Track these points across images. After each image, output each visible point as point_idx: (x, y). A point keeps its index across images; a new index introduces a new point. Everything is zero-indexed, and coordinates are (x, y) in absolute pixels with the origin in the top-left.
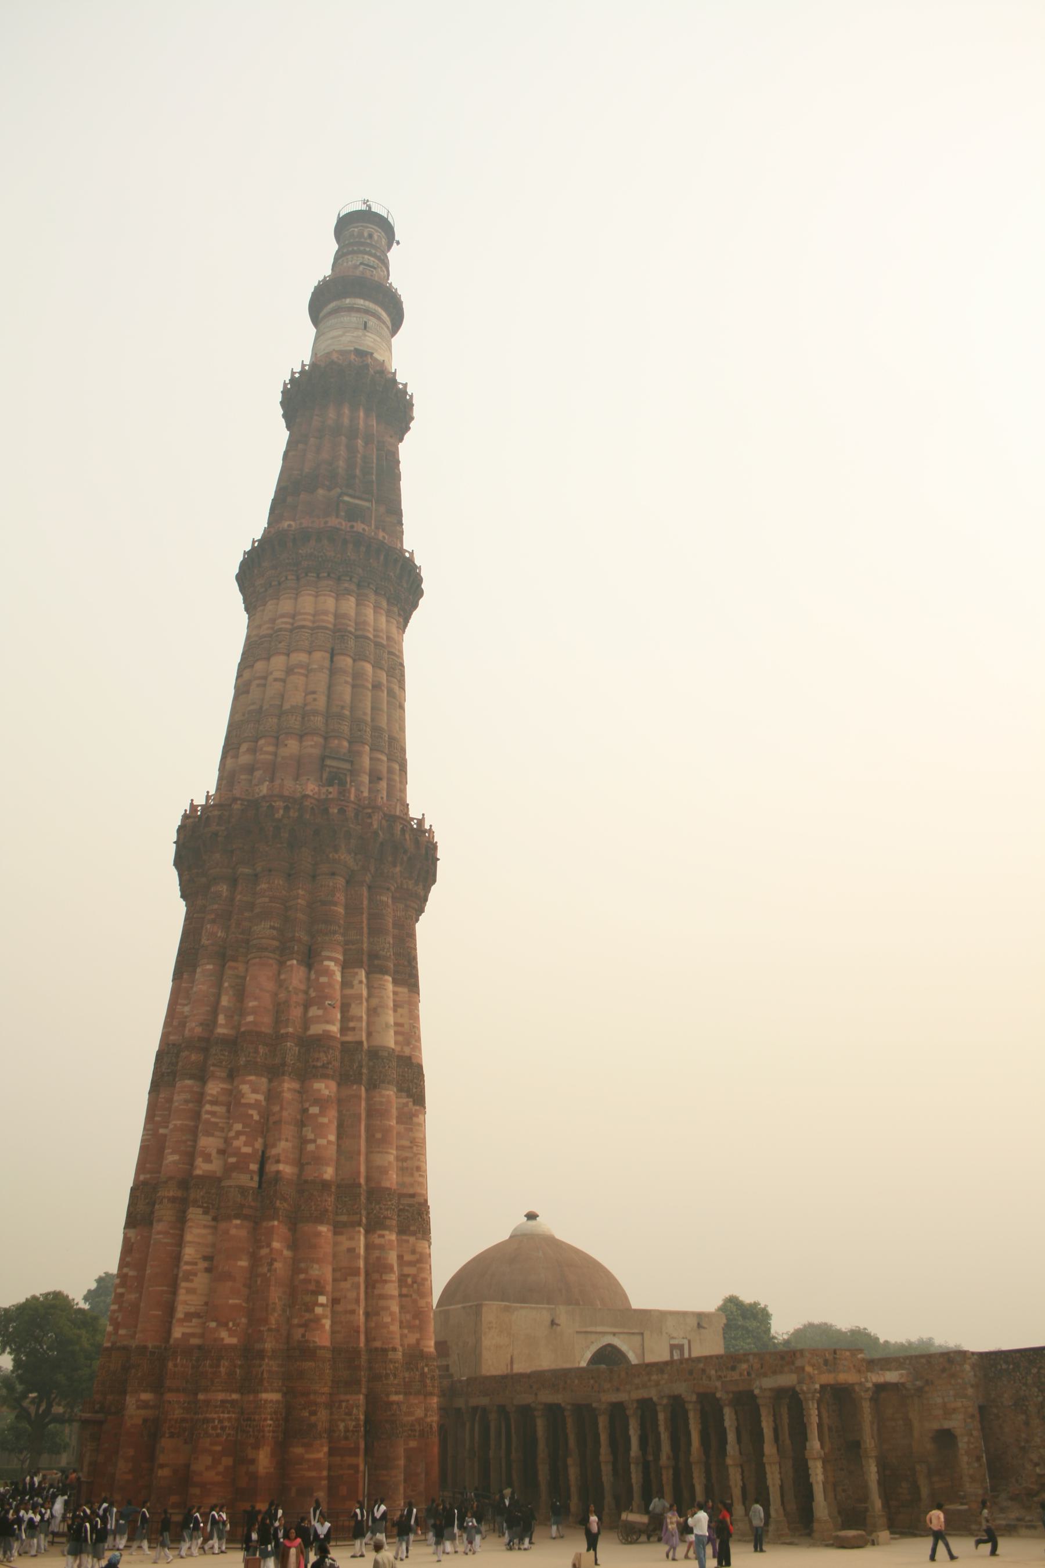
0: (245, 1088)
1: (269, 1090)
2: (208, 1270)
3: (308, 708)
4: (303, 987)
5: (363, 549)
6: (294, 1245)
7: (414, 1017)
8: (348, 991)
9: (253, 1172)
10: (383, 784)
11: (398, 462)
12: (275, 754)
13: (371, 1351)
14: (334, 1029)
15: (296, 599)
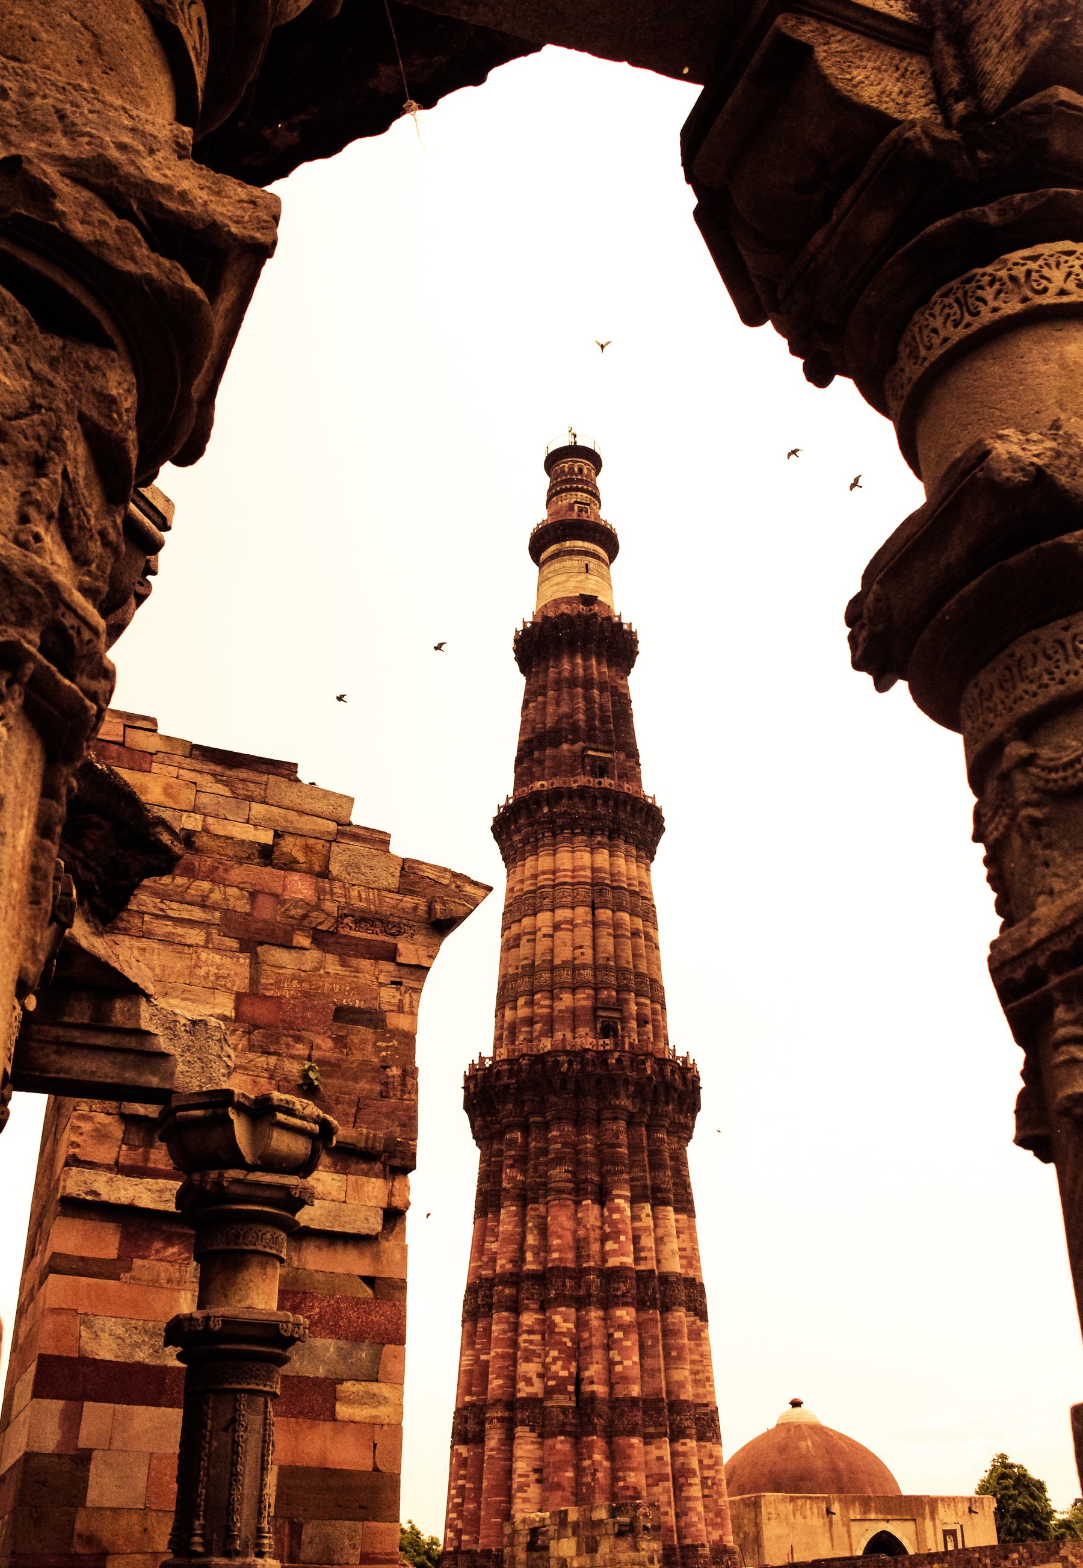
0: (557, 1319)
1: (578, 1319)
2: (538, 1481)
3: (576, 962)
4: (598, 1224)
5: (611, 803)
6: (612, 1455)
7: (693, 1240)
8: (637, 1224)
9: (570, 1393)
10: (650, 1027)
11: (630, 701)
12: (551, 1007)
13: (683, 1548)
14: (629, 1260)
15: (554, 855)
